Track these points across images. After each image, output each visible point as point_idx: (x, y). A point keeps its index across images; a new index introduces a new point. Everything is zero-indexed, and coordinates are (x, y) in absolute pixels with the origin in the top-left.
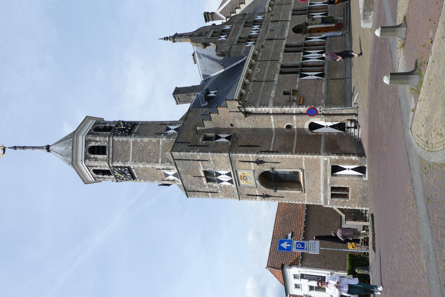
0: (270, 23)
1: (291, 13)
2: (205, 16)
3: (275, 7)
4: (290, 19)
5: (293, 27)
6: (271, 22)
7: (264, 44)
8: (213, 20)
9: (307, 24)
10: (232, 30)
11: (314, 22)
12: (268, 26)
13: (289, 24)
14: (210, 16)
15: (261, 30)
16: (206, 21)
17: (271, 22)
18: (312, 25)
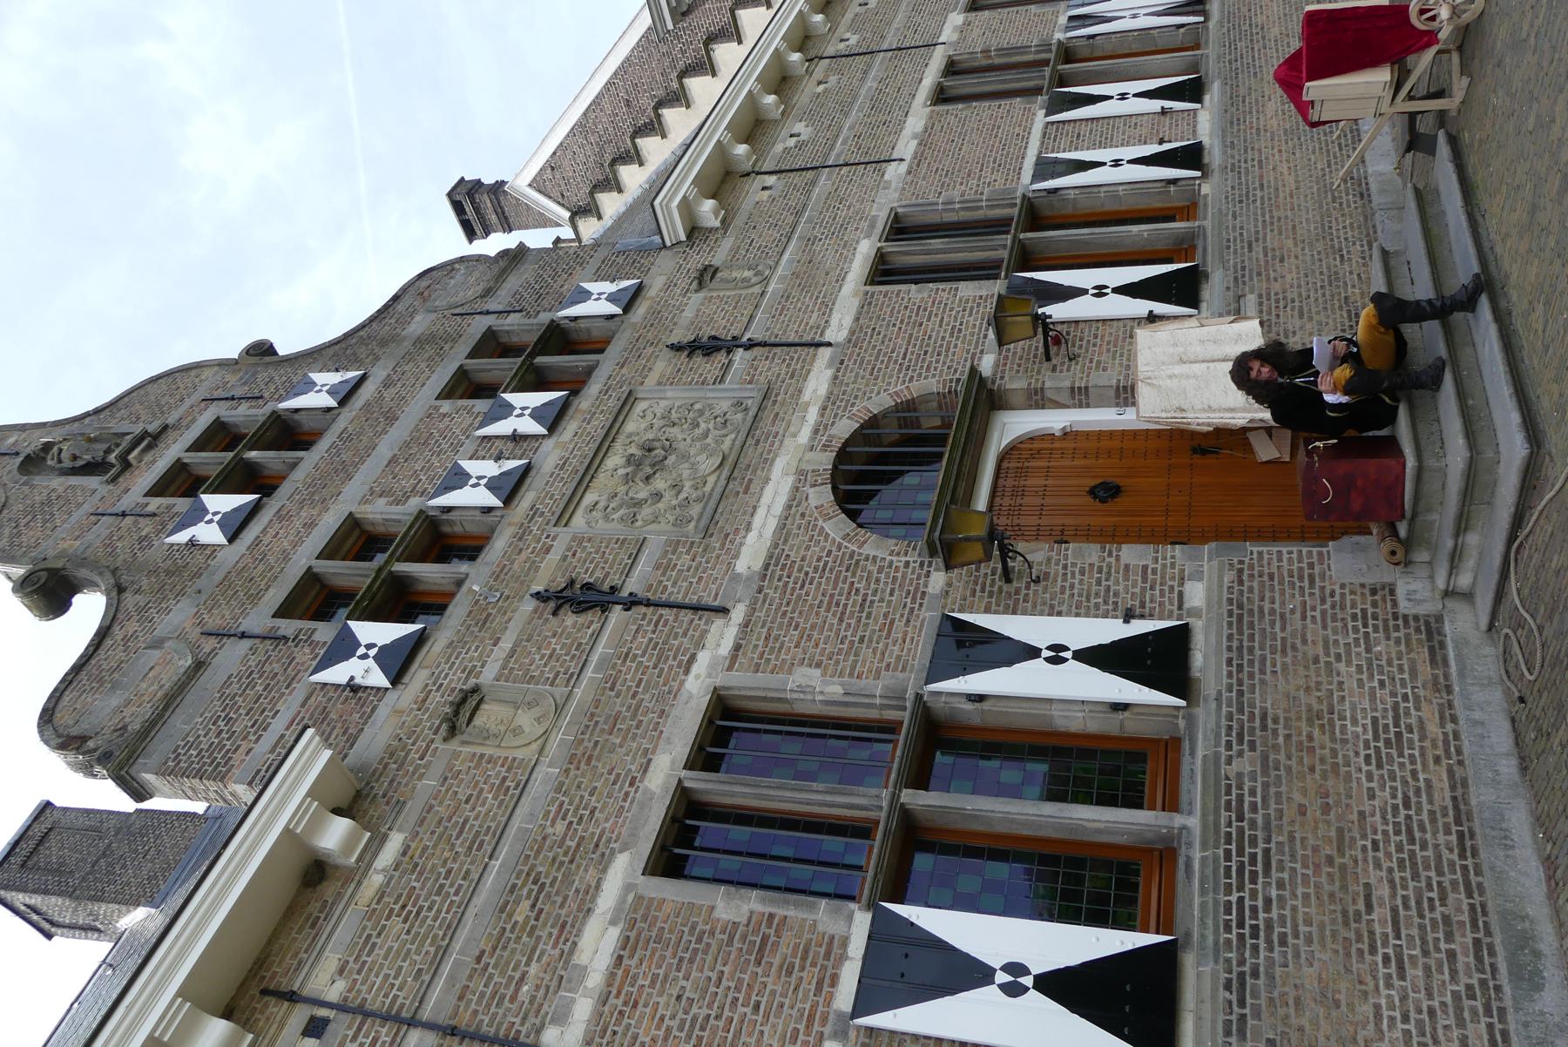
0: (663, 364)
1: (865, 249)
2: (458, 208)
3: (754, 194)
4: (838, 330)
5: (844, 428)
6: (676, 348)
7: (487, 676)
8: (508, 228)
9: (985, 399)
10: (347, 414)
11: (1055, 381)
12: (629, 400)
13: (818, 382)
14: (486, 202)
15: (550, 456)
16: (471, 234)
17: (676, 348)
18: (1037, 399)
